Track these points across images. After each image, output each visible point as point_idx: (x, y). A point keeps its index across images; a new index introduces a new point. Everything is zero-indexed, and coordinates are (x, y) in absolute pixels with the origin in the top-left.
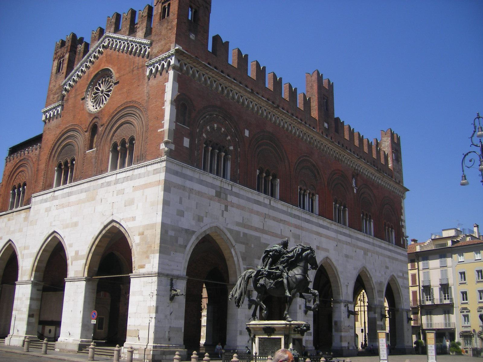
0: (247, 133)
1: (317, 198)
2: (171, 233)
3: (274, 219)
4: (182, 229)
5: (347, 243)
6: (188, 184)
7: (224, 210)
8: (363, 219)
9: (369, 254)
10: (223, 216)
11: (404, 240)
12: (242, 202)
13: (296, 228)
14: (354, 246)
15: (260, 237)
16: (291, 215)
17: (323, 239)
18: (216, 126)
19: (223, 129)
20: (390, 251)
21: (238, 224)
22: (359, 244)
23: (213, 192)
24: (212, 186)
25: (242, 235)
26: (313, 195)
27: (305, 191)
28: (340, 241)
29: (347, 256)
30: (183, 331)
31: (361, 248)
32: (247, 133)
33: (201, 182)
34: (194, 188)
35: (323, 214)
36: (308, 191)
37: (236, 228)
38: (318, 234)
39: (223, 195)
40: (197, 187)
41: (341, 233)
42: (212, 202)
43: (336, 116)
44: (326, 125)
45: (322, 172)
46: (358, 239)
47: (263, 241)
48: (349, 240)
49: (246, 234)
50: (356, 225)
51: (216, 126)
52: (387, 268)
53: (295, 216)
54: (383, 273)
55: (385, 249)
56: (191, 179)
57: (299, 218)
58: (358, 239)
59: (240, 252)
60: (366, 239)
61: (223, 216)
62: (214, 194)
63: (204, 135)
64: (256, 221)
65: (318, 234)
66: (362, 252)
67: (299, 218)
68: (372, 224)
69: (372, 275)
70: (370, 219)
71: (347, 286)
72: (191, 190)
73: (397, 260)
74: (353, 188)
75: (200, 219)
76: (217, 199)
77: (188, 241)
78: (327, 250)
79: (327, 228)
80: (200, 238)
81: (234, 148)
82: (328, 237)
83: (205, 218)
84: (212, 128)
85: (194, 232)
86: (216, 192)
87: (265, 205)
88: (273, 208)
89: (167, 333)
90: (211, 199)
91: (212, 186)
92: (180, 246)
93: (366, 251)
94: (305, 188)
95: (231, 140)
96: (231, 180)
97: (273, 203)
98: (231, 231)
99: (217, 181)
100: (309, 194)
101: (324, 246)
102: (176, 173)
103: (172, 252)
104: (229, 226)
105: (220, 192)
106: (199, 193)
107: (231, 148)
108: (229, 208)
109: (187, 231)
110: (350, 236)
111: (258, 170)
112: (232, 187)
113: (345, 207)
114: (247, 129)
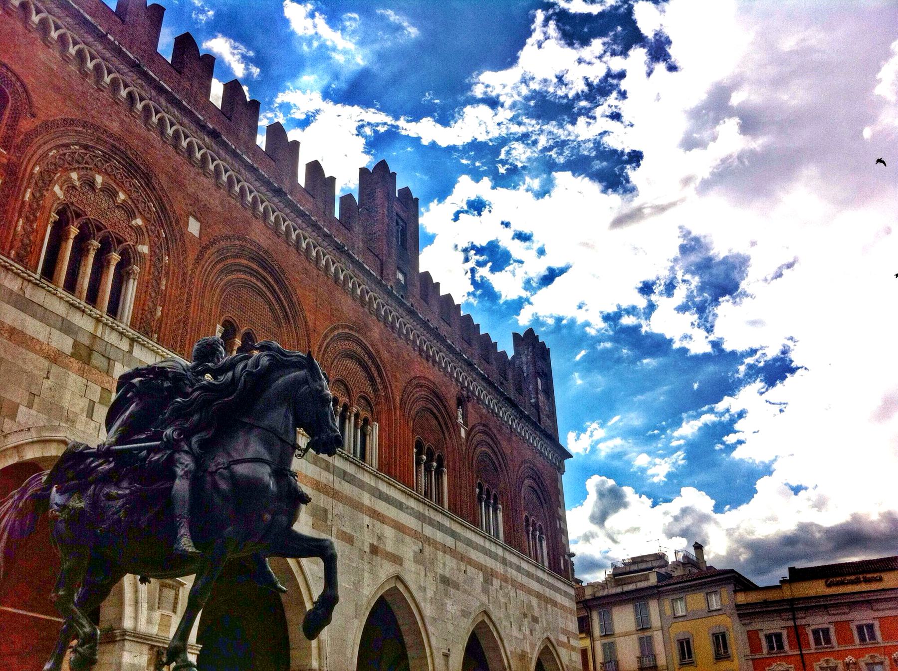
0: (194, 227)
1: (375, 430)
5: (446, 549)
8: (480, 501)
9: (496, 583)
11: (566, 562)
13: (319, 490)
14: (462, 558)
17: (389, 532)
18: (99, 179)
19: (122, 196)
20: (539, 581)
23: (66, 344)
24: (67, 328)
26: (366, 422)
27: (346, 408)
28: (428, 540)
29: (445, 581)
31: (480, 567)
32: (194, 227)
35: (389, 468)
36: (355, 410)
41: (431, 522)
42: (55, 369)
43: (422, 270)
44: (400, 276)
45: (389, 374)
46: (469, 543)
48: (449, 541)
50: (465, 511)
52: (535, 620)
54: (528, 632)
55: (529, 575)
60: (487, 545)
63: (57, 189)
65: (375, 515)
66: (481, 577)
68: (500, 515)
69: (503, 634)
70: (496, 503)
71: (446, 656)
73: (555, 604)
74: (457, 427)
76: (76, 364)
78: (397, 560)
79: (400, 506)
81: (151, 248)
82: (399, 527)
83: (22, 409)
86: (76, 345)
91: (67, 328)
93: (489, 575)
95: (144, 230)
96: (132, 325)
100: (357, 416)
101: (390, 547)
105: (91, 350)
107: (144, 249)
110: (453, 534)
111: (219, 327)
112: (131, 346)
113: (440, 465)
114: (197, 219)
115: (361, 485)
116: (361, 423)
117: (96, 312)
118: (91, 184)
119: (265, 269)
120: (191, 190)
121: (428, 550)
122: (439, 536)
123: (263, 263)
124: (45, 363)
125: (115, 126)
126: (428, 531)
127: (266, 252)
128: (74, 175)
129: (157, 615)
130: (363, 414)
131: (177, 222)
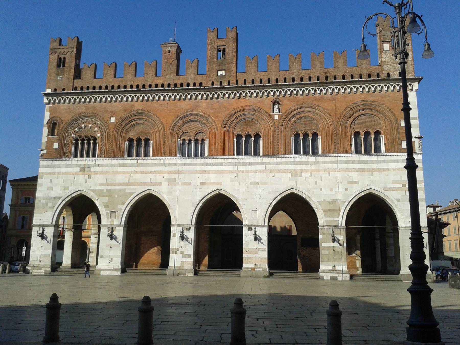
2: (43, 201)
3: (142, 172)
4: (51, 198)
6: (57, 170)
7: (87, 178)
10: (86, 182)
12: (105, 169)
15: (125, 189)
16: (164, 165)
21: (101, 184)
22: (281, 167)
24: (77, 166)
25: (105, 191)
27: (190, 140)
30: (51, 256)
32: (113, 120)
33: (67, 166)
34: (62, 171)
36: (194, 140)
37: (100, 188)
38: (203, 172)
39: (86, 169)
40: (63, 170)
41: (244, 164)
47: (127, 191)
48: (263, 167)
49: (110, 189)
51: (83, 126)
53: (169, 165)
56: (59, 166)
57: (175, 165)
58: (280, 163)
59: (103, 203)
61: (86, 182)
62: (79, 170)
64: (120, 178)
65: (203, 172)
66: (289, 175)
67: (175, 165)
72: (59, 173)
75: (66, 189)
77: (56, 203)
79: (221, 164)
80: (67, 200)
84: (80, 128)
85: (60, 197)
87: (132, 165)
88: (142, 165)
89: (39, 258)
90: (76, 174)
91: (77, 166)
92: (50, 207)
93: (295, 174)
94: (187, 139)
97: (140, 161)
98: (94, 191)
99: (82, 162)
101: (213, 181)
102: (48, 166)
103: (43, 212)
104: (92, 188)
105: (84, 168)
106: (66, 173)
107: (99, 135)
108: (92, 176)
109: (55, 198)
110: (262, 163)
115: (195, 165)
116: (200, 142)
117: (84, 159)
118: (82, 128)
119: (142, 115)
120: (109, 110)
121: (240, 175)
122: (250, 168)
123: (141, 115)
124: (74, 176)
125: (84, 110)
126: (241, 168)
127: (141, 110)
128: (76, 129)
129: (110, 220)
130: (199, 138)
131: (106, 122)
